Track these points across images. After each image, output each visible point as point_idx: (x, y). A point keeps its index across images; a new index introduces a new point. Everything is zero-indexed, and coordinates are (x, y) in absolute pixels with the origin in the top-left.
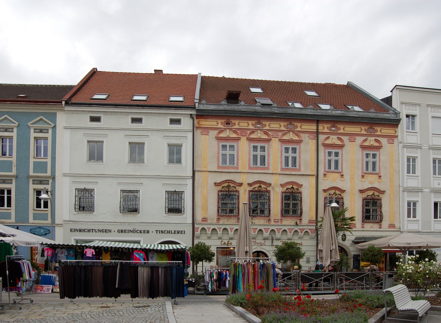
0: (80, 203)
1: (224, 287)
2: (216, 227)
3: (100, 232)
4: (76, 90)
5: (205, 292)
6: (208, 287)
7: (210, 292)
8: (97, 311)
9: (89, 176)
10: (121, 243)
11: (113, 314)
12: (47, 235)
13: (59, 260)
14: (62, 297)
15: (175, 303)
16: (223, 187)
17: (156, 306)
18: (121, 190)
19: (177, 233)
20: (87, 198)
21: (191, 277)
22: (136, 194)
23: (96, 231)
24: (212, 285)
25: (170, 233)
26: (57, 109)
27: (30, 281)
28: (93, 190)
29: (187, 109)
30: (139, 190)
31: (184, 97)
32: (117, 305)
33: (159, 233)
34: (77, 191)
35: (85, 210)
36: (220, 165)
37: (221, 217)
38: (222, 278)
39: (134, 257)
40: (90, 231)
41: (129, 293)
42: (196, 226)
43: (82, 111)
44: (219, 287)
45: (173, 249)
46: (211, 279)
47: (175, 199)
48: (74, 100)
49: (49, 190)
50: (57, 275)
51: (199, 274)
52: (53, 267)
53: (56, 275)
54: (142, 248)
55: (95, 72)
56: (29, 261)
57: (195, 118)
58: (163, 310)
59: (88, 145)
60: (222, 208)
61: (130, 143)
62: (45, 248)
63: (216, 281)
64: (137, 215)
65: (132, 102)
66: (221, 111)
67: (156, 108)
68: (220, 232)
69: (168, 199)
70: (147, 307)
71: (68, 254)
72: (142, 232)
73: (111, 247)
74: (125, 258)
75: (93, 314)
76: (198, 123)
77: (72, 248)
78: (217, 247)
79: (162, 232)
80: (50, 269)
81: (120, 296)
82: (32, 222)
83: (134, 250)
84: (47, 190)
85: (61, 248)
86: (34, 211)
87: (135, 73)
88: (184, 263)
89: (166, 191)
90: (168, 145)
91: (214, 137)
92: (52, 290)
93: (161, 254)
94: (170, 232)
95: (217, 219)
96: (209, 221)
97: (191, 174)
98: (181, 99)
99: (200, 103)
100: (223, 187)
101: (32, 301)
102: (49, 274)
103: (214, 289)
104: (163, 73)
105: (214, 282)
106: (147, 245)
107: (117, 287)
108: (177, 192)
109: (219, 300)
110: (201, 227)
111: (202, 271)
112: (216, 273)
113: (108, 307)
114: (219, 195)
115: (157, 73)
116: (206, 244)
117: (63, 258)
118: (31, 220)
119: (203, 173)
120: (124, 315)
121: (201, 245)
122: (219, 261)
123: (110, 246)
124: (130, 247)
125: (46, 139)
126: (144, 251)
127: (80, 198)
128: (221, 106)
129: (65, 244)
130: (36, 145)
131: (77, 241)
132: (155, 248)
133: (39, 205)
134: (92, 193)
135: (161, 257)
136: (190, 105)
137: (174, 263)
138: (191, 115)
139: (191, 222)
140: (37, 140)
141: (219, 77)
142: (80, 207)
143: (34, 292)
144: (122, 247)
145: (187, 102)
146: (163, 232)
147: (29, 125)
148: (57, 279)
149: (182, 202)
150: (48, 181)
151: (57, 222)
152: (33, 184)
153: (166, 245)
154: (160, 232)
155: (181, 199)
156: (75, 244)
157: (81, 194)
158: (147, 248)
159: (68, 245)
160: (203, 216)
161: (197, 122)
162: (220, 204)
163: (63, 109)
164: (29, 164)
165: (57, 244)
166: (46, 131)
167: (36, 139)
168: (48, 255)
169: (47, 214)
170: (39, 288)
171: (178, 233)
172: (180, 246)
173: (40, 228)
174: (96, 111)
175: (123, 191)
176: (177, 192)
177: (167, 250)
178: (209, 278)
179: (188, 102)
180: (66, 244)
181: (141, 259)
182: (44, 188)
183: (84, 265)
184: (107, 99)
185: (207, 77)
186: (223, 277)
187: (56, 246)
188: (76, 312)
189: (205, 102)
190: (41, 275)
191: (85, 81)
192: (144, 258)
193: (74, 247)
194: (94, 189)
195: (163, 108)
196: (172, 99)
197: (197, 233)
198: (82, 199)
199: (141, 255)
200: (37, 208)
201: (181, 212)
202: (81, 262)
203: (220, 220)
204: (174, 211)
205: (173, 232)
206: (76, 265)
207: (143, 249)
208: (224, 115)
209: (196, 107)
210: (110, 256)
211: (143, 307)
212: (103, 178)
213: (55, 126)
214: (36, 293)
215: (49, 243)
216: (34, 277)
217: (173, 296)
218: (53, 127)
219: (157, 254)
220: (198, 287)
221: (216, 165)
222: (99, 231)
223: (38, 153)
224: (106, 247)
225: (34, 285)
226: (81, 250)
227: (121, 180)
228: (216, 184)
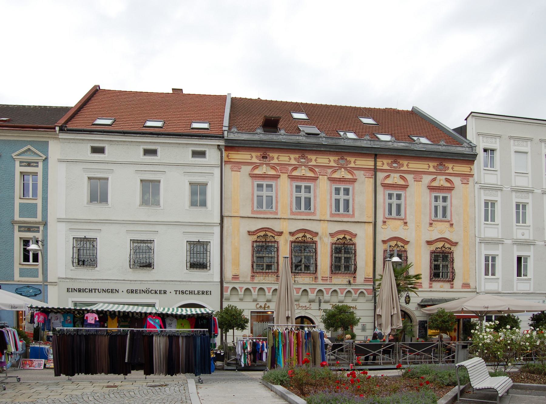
0: (80, 256)
1: (260, 361)
2: (249, 286)
3: (105, 292)
4: (73, 113)
5: (237, 368)
7: (243, 368)
8: (102, 391)
10: (131, 307)
11: (122, 395)
12: (37, 295)
13: (53, 327)
14: (57, 374)
15: (200, 382)
16: (259, 236)
17: (176, 385)
18: (131, 240)
19: (201, 293)
20: (87, 249)
21: (219, 348)
22: (150, 245)
23: (100, 291)
25: (192, 294)
26: (49, 137)
27: (17, 354)
28: (95, 240)
30: (154, 240)
31: (210, 124)
32: (127, 383)
33: (179, 294)
34: (76, 240)
35: (85, 264)
36: (255, 209)
37: (256, 274)
38: (258, 350)
39: (148, 324)
40: (92, 291)
41: (142, 370)
42: (225, 285)
43: (80, 139)
44: (254, 361)
45: (197, 314)
46: (244, 351)
48: (70, 126)
49: (40, 239)
50: (51, 347)
51: (229, 345)
52: (45, 337)
53: (49, 346)
54: (157, 313)
55: (97, 91)
56: (15, 329)
57: (223, 150)
58: (184, 390)
59: (88, 183)
60: (258, 262)
61: (141, 181)
62: (35, 313)
63: (250, 354)
64: (152, 271)
66: (256, 142)
68: (255, 292)
69: (190, 251)
70: (165, 386)
71: (64, 320)
72: (158, 292)
73: (119, 312)
74: (136, 326)
75: (97, 395)
76: (228, 156)
77: (70, 312)
78: (251, 312)
79: (183, 292)
80: (42, 339)
81: (130, 373)
83: (147, 315)
84: (37, 239)
85: (56, 313)
86: (21, 265)
87: (148, 93)
88: (210, 331)
89: (187, 241)
90: (190, 183)
92: (45, 365)
93: (181, 320)
94: (193, 293)
95: (251, 276)
96: (241, 279)
97: (218, 221)
98: (206, 126)
99: (230, 131)
100: (258, 237)
101: (19, 380)
103: (248, 364)
104: (184, 93)
105: (248, 355)
106: (164, 309)
107: (126, 361)
108: (201, 243)
109: (254, 377)
110: (231, 286)
111: (233, 342)
112: (250, 343)
113: (116, 386)
114: (253, 247)
118: (17, 277)
119: (233, 218)
120: (135, 396)
121: (232, 309)
122: (254, 329)
123: (117, 310)
124: (143, 311)
125: (35, 174)
126: (160, 317)
127: (78, 250)
128: (256, 135)
129: (61, 308)
130: (22, 182)
131: (75, 304)
132: (174, 313)
133: (26, 259)
134: (95, 243)
135: (182, 324)
136: (217, 133)
137: (197, 331)
138: (219, 146)
139: (219, 280)
140: (24, 175)
142: (79, 261)
143: (22, 367)
144: (132, 311)
145: (214, 130)
146: (184, 292)
148: (51, 351)
149: (208, 255)
150: (39, 227)
151: (49, 280)
152: (19, 231)
153: (188, 309)
154: (181, 293)
155: (207, 252)
156: (74, 308)
157: (80, 244)
158: (164, 312)
159: (64, 309)
160: (234, 273)
161: (226, 155)
162: (255, 258)
163: (57, 136)
165: (50, 307)
166: (35, 164)
167: (23, 174)
168: (38, 322)
169: (37, 269)
170: (28, 362)
171: (202, 294)
172: (205, 310)
173: (28, 287)
174: (99, 140)
175: (133, 241)
176: (201, 243)
177: (190, 315)
178: (241, 350)
180: (62, 308)
181: (157, 326)
182: (33, 236)
183: (85, 334)
184: (112, 124)
185: (238, 98)
186: (259, 349)
187: (50, 310)
188: (75, 393)
189: (236, 130)
190: (30, 346)
191: (84, 101)
194: (97, 238)
195: (184, 137)
196: (195, 125)
197: (226, 294)
198: (82, 251)
199: (157, 321)
200: (24, 261)
201: (207, 268)
202: (81, 330)
203: (254, 278)
204: (198, 266)
205: (196, 292)
206: (74, 334)
207: (159, 314)
208: (260, 146)
209: (225, 136)
210: (118, 322)
211: (159, 386)
212: (107, 225)
213: (46, 159)
214: (24, 369)
215: (40, 306)
216: (21, 349)
217: (196, 373)
218: (44, 160)
219: (177, 320)
220: (228, 361)
222: (103, 292)
223: (25, 192)
224: (113, 311)
225: (22, 360)
226: (81, 314)
227: (131, 228)
228: (250, 233)
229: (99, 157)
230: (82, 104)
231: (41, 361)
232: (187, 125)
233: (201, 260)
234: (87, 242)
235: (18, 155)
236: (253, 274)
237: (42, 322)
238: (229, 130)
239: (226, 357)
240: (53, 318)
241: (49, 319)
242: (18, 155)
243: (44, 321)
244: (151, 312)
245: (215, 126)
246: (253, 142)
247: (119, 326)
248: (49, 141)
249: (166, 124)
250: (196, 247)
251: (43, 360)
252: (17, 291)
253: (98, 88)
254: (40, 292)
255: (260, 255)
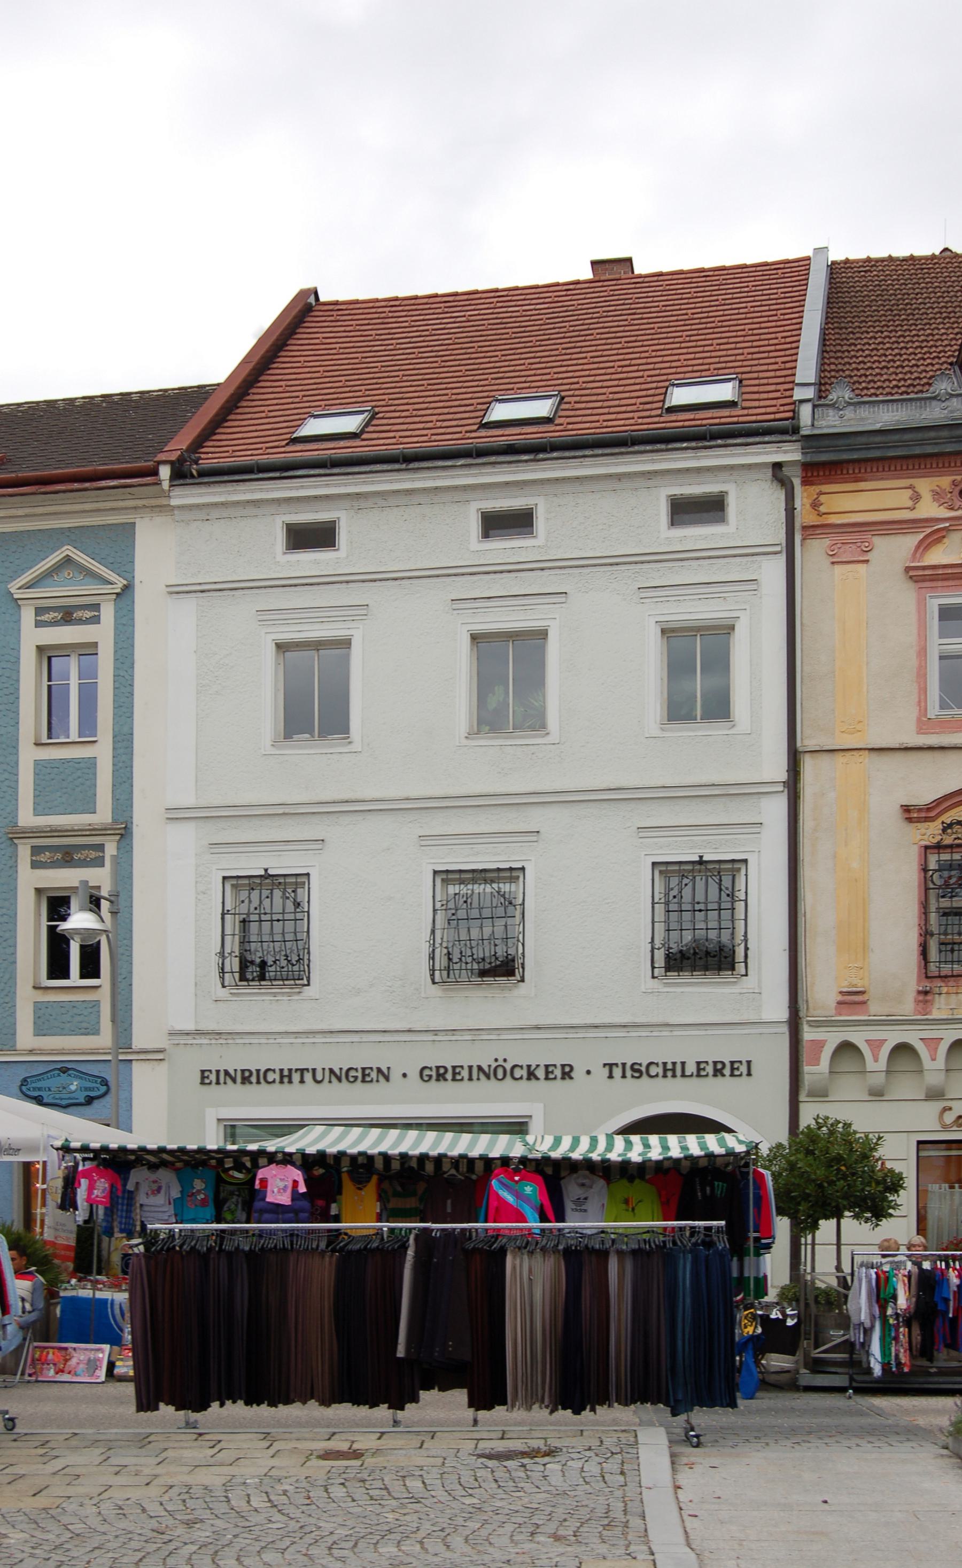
2: (912, 1037)
4: (222, 408)
6: (868, 1354)
9: (284, 814)
10: (431, 1135)
12: (96, 1101)
15: (693, 1439)
16: (950, 826)
20: (275, 917)
24: (888, 1339)
26: (135, 508)
28: (300, 880)
29: (757, 439)
31: (741, 381)
34: (232, 885)
36: (934, 710)
38: (941, 1307)
43: (248, 502)
44: (925, 1351)
46: (883, 1309)
47: (702, 900)
48: (211, 458)
49: (104, 893)
52: (116, 1259)
54: (530, 1156)
55: (308, 309)
57: (797, 482)
60: (946, 934)
62: (81, 1168)
63: (908, 1323)
65: (483, 433)
67: (600, 451)
68: (934, 1059)
69: (667, 903)
71: (182, 1192)
73: (386, 1157)
74: (449, 1210)
76: (815, 505)
77: (204, 1163)
82: (29, 1047)
84: (94, 892)
85: (153, 1167)
86: (39, 992)
87: (497, 290)
89: (654, 864)
90: (663, 631)
91: (899, 569)
92: (111, 1366)
93: (624, 1182)
95: (919, 992)
96: (876, 1009)
97: (780, 772)
98: (724, 392)
99: (822, 402)
100: (947, 828)
102: (94, 1289)
104: (637, 272)
105: (897, 1327)
108: (710, 866)
109: (921, 1421)
110: (833, 1039)
112: (909, 1277)
114: (925, 870)
115: (607, 277)
116: (854, 1128)
117: (160, 1215)
118: (25, 1037)
119: (840, 759)
121: (832, 1132)
125: (89, 650)
128: (934, 403)
129: (170, 1147)
130: (45, 683)
132: (595, 1156)
133: (58, 968)
134: (302, 894)
135: (627, 1201)
136: (772, 417)
138: (777, 466)
139: (782, 1014)
140: (49, 658)
141: (921, 258)
143: (30, 1375)
144: (434, 1153)
145: (756, 404)
147: (13, 591)
149: (736, 917)
150: (101, 847)
151: (139, 1040)
152: (35, 865)
153: (654, 1139)
154: (629, 1073)
157: (250, 902)
158: (556, 1155)
159: (182, 1150)
160: (846, 983)
161: (808, 502)
162: (933, 917)
163: (164, 501)
164: (17, 775)
166: (88, 614)
167: (47, 654)
168: (91, 1202)
169: (96, 1004)
170: (50, 1356)
172: (722, 1143)
173: (64, 1070)
174: (316, 497)
176: (710, 866)
178: (870, 1306)
179: (762, 403)
181: (529, 1212)
182: (81, 882)
184: (362, 432)
185: (857, 261)
186: (947, 1300)
187: (133, 1157)
189: (847, 395)
190: (62, 1294)
191: (262, 357)
192: (542, 1205)
193: (213, 1158)
195: (636, 448)
196: (681, 396)
198: (254, 927)
199: (529, 1189)
200: (52, 975)
201: (733, 969)
203: (931, 1002)
208: (949, 448)
209: (802, 424)
210: (380, 1198)
213: (128, 588)
214: (37, 1381)
215: (95, 1145)
218: (117, 594)
221: (910, 715)
223: (54, 719)
228: (911, 814)
229: (316, 562)
230: (254, 369)
231: (98, 1350)
232: (650, 399)
233: (713, 935)
234: (272, 890)
235: (29, 586)
236: (928, 985)
237: (101, 1203)
238: (820, 397)
239: (807, 1334)
240: (144, 1188)
241: (130, 1192)
242: (29, 586)
243: (111, 1198)
244: (506, 1153)
245: (762, 389)
246: (920, 435)
247: (384, 1217)
248: (137, 521)
249: (567, 406)
250: (690, 885)
251: (104, 1346)
252: (24, 1088)
253: (312, 300)
254: (105, 1087)
255: (955, 905)
